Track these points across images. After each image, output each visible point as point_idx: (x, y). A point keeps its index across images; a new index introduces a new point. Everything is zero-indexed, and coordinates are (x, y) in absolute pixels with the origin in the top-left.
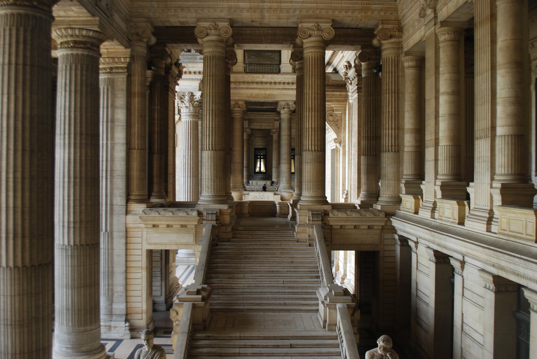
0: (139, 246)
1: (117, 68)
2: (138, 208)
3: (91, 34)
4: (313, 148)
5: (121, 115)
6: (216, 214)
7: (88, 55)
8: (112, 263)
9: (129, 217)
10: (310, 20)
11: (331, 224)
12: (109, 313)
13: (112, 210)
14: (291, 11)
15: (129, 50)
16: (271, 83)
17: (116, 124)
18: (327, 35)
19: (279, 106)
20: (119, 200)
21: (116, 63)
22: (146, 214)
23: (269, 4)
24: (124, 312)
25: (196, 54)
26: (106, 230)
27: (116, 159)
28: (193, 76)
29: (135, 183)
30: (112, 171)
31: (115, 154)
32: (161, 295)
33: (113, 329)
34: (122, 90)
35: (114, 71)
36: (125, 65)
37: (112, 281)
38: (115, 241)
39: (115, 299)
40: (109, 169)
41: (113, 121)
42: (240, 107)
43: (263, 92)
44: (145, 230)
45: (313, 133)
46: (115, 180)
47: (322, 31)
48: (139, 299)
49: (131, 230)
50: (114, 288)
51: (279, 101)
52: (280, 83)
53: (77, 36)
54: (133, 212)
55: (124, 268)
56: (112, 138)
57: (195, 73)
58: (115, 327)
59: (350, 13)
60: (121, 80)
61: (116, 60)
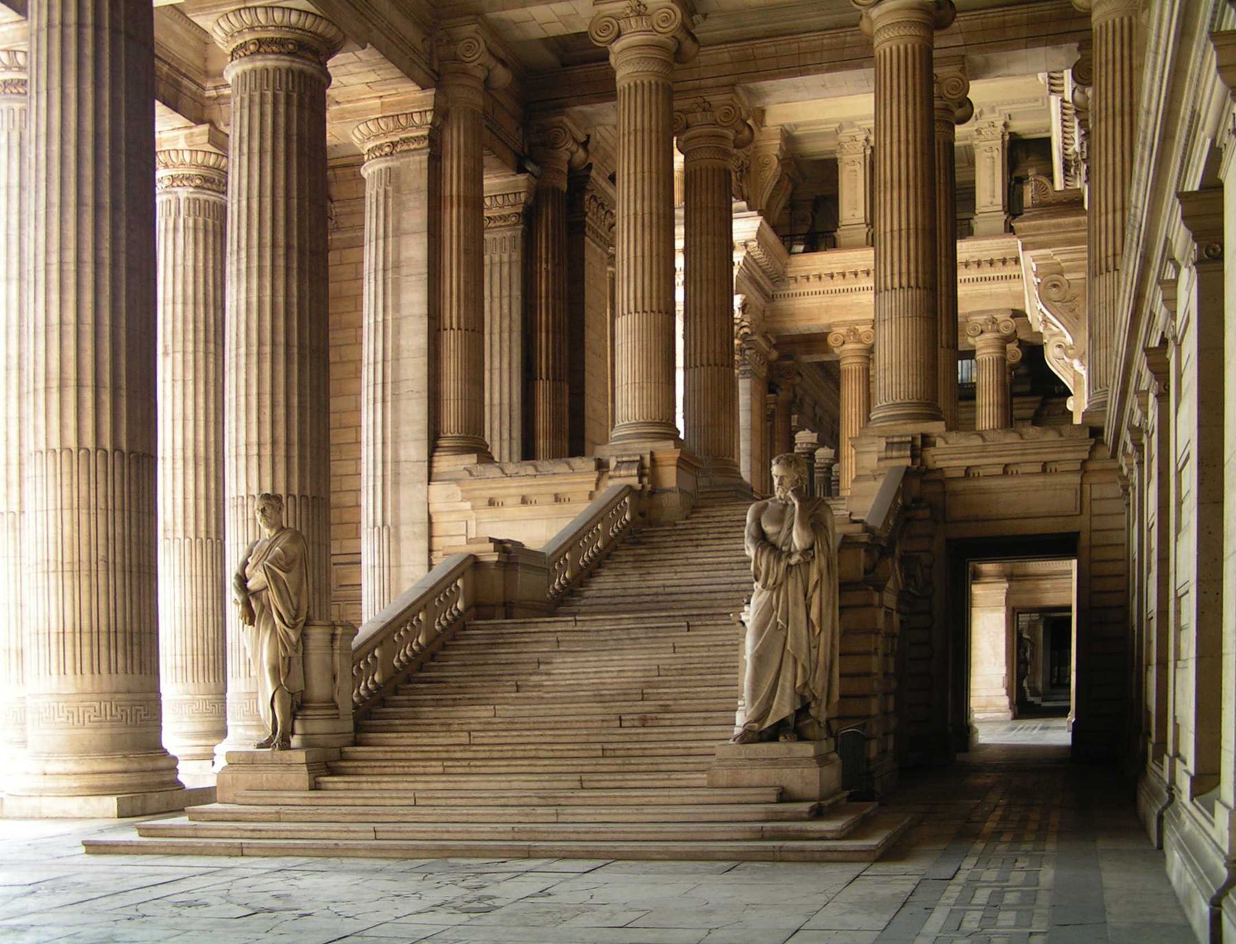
3: (294, 17)
7: (289, 71)
9: (436, 487)
11: (939, 464)
13: (396, 474)
15: (431, 93)
17: (404, 271)
20: (414, 449)
21: (404, 129)
27: (405, 354)
30: (396, 382)
31: (403, 342)
34: (418, 190)
35: (399, 148)
40: (389, 380)
41: (397, 266)
42: (860, 342)
46: (403, 404)
53: (264, 28)
56: (397, 307)
61: (403, 120)
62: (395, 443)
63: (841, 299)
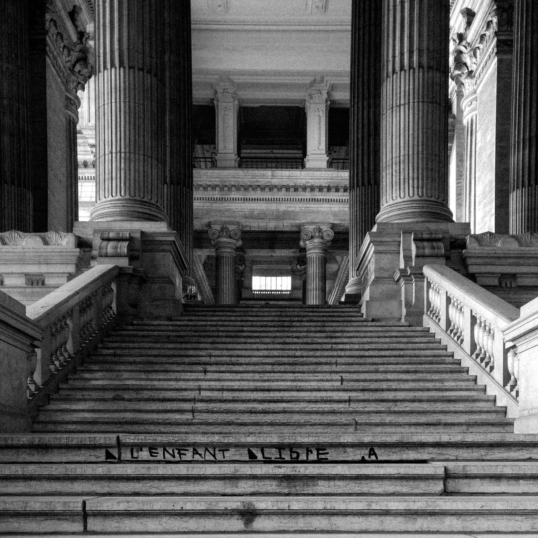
6: (131, 239)
16: (288, 188)
19: (303, 235)
43: (273, 207)
51: (303, 224)
52: (304, 188)
63: (216, 206)
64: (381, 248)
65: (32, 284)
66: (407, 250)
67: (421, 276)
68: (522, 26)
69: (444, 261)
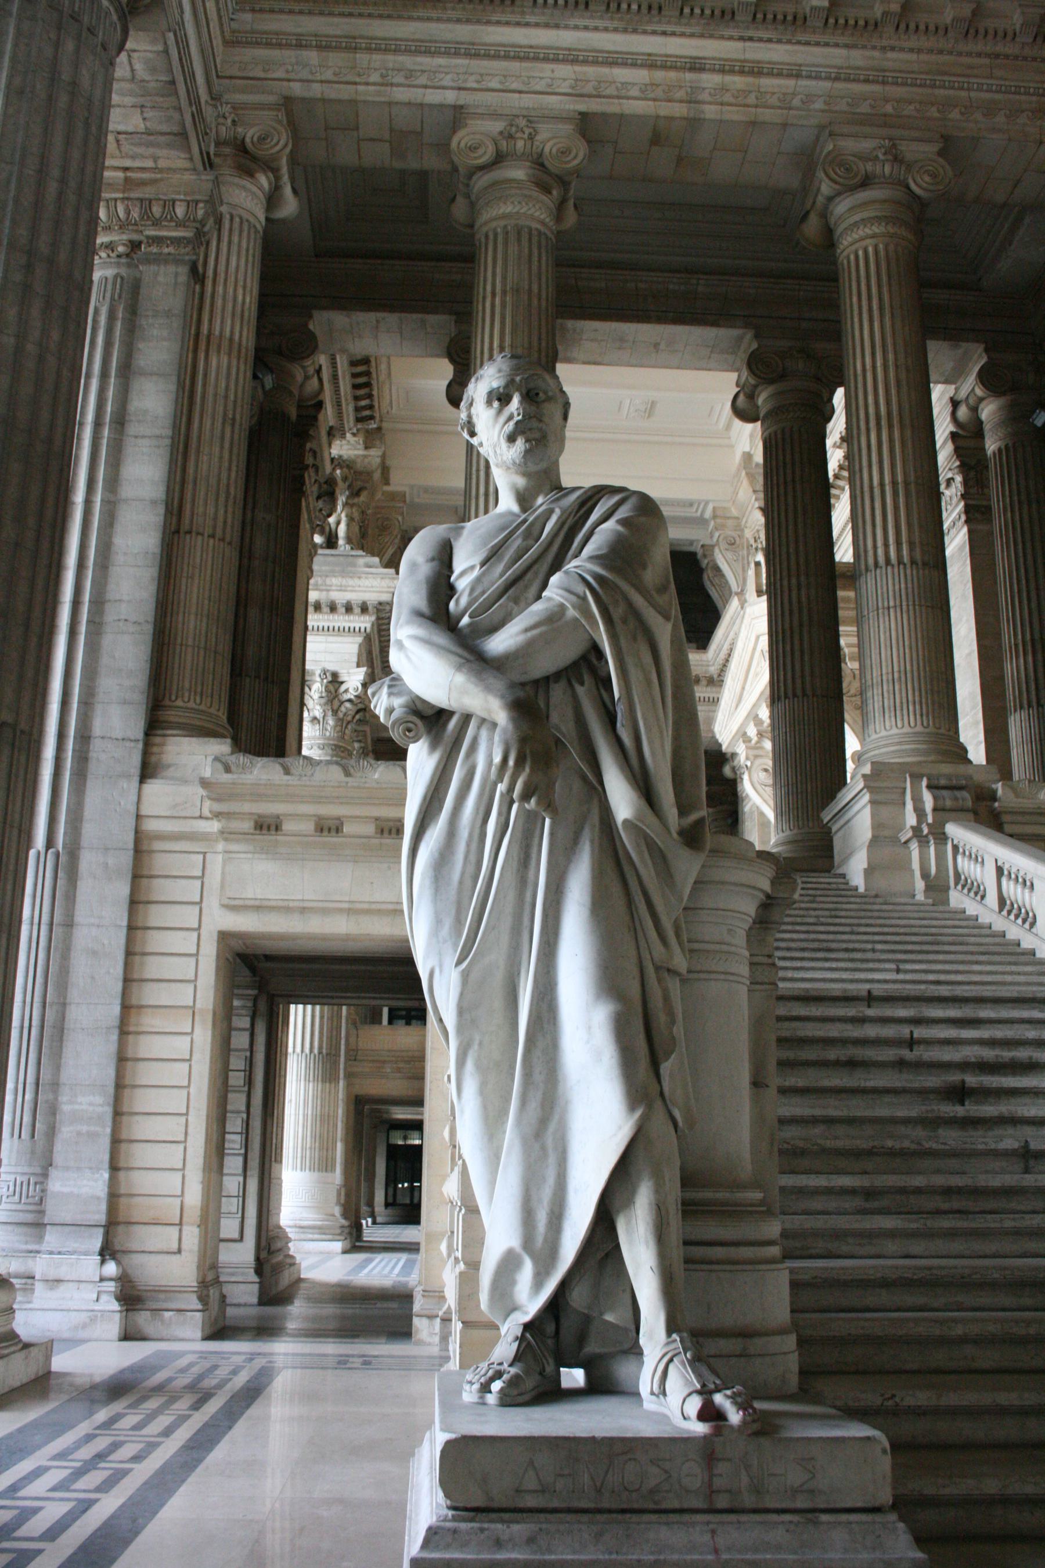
0: (188, 916)
1: (158, 240)
2: (196, 757)
4: (905, 552)
5: (153, 402)
8: (63, 987)
9: (152, 788)
10: (868, 130)
12: (29, 1218)
14: (796, 102)
17: (132, 429)
18: (927, 178)
20: (119, 719)
21: (156, 223)
22: (228, 769)
23: (717, 78)
24: (100, 1215)
25: (354, 553)
26: (50, 843)
27: (119, 558)
28: (340, 620)
29: (188, 660)
30: (99, 603)
31: (119, 541)
32: (241, 1239)
33: (39, 1286)
34: (168, 314)
36: (188, 234)
37: (57, 1068)
38: (85, 886)
39: (61, 1153)
40: (86, 597)
41: (120, 421)
44: (220, 846)
45: (902, 499)
46: (107, 640)
47: (909, 167)
48: (173, 1156)
49: (158, 845)
50: (64, 1098)
54: (171, 772)
55: (117, 1009)
56: (113, 482)
57: (349, 609)
58: (56, 1282)
59: (1000, 119)
60: (166, 286)
62: (87, 704)
64: (878, 797)
65: (322, 830)
66: (918, 801)
67: (942, 838)
68: (1003, 496)
69: (971, 815)
